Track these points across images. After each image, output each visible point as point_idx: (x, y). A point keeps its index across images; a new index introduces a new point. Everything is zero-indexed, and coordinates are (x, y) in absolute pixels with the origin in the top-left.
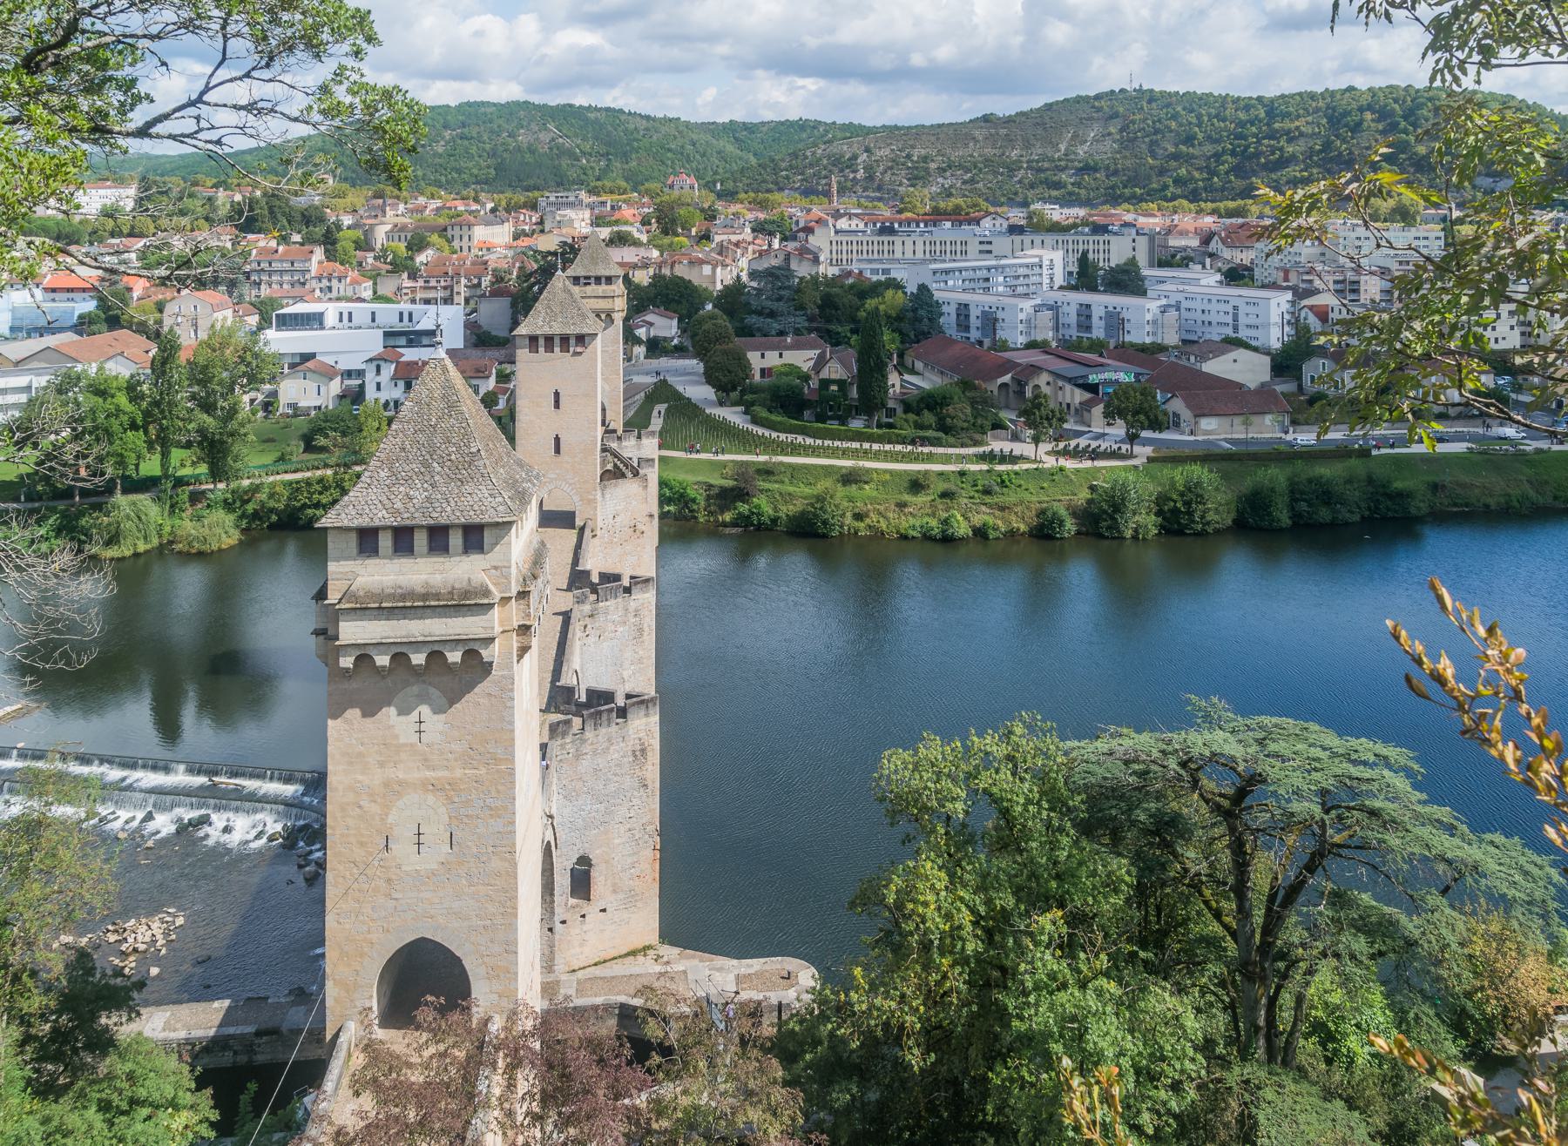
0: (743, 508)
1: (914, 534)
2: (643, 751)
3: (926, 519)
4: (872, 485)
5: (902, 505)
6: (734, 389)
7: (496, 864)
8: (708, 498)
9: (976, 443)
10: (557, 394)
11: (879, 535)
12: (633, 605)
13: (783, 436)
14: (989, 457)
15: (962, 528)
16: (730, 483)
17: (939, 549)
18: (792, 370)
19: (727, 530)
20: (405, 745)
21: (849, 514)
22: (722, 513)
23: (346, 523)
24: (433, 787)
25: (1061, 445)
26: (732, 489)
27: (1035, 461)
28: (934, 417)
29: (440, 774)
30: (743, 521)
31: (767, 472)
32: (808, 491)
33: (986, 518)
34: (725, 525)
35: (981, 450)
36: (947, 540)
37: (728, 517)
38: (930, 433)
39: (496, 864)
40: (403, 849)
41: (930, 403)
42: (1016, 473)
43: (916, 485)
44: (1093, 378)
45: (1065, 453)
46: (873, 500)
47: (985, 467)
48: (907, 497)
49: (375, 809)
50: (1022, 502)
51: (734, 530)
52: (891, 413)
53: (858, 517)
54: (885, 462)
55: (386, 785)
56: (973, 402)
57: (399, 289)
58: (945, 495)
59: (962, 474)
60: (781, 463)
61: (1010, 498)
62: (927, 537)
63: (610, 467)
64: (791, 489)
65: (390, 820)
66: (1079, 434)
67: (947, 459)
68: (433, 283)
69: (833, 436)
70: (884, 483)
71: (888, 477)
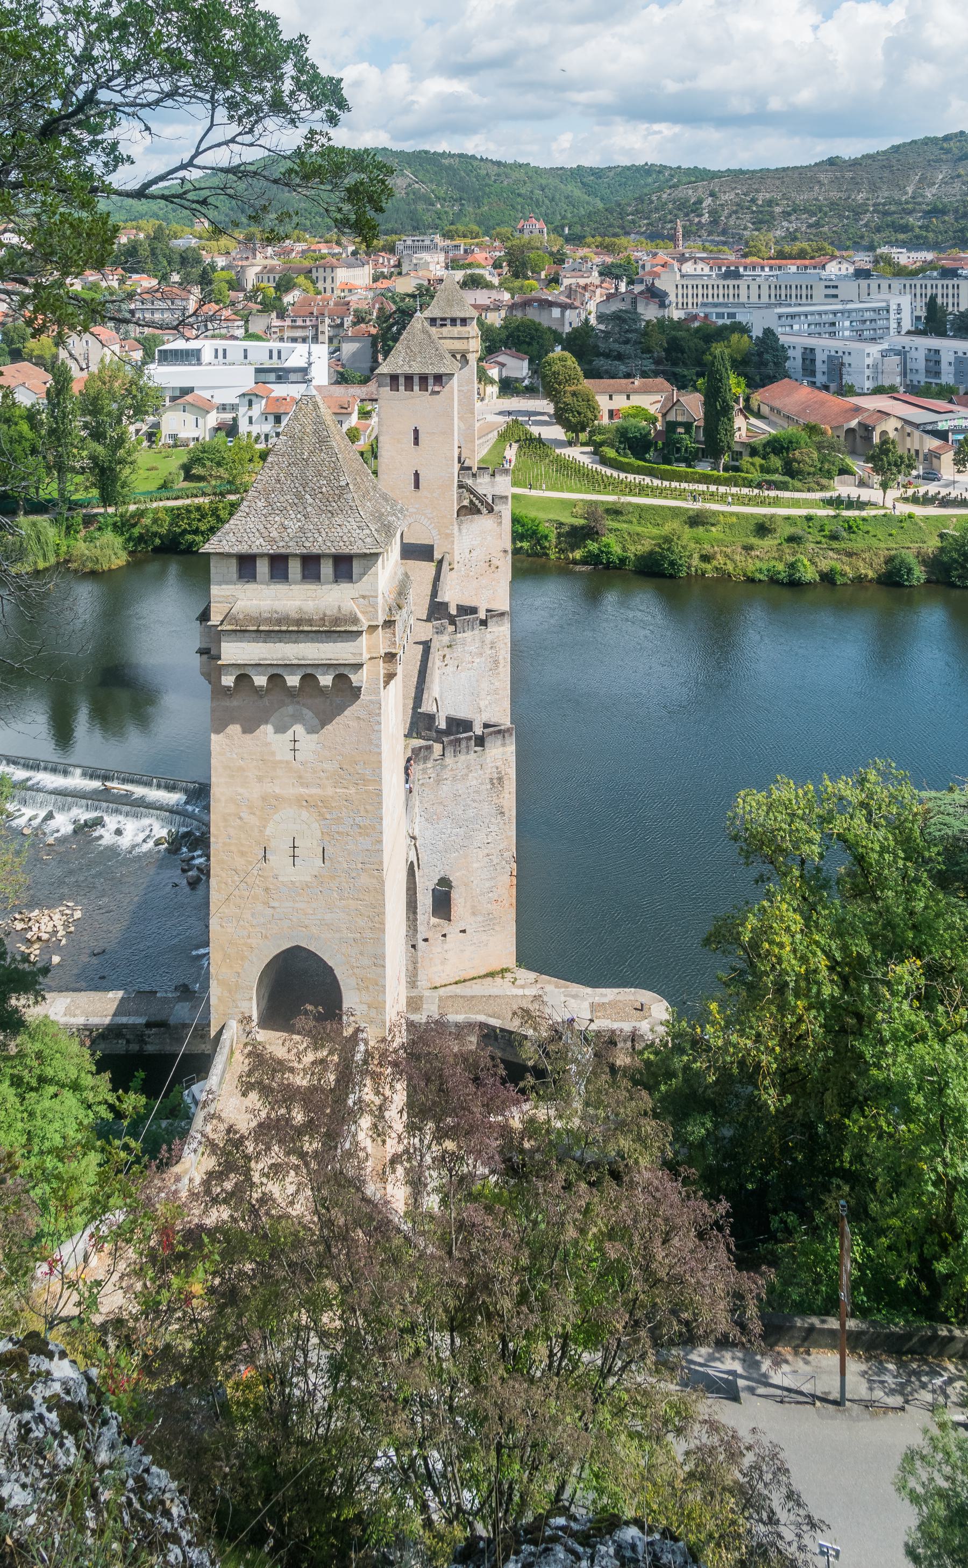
0: (593, 546)
1: (762, 577)
2: (500, 779)
3: (773, 563)
4: (719, 527)
5: (748, 548)
6: (583, 429)
7: (364, 880)
8: (559, 535)
9: (823, 488)
10: (416, 431)
11: (724, 577)
12: (489, 637)
13: (631, 477)
14: (836, 502)
15: (809, 574)
16: (582, 522)
17: (786, 594)
18: (640, 412)
19: (578, 568)
20: (281, 762)
21: (696, 556)
22: (573, 551)
23: (227, 549)
24: (305, 803)
25: (910, 492)
26: (582, 528)
27: (883, 507)
28: (784, 461)
29: (314, 791)
30: (592, 559)
31: (615, 512)
32: (655, 531)
34: (575, 562)
35: (827, 495)
36: (794, 584)
37: (578, 554)
38: (776, 477)
39: (364, 880)
40: (279, 860)
41: (777, 447)
42: (864, 519)
43: (762, 529)
44: (942, 426)
45: (915, 500)
46: (720, 543)
47: (832, 512)
49: (253, 820)
50: (870, 549)
51: (584, 568)
52: (737, 456)
53: (706, 558)
54: (731, 503)
55: (264, 799)
56: (819, 447)
58: (792, 539)
59: (809, 518)
60: (630, 504)
61: (858, 543)
62: (774, 581)
63: (466, 503)
64: (639, 529)
67: (796, 503)
69: (680, 478)
70: (731, 527)
71: (734, 520)
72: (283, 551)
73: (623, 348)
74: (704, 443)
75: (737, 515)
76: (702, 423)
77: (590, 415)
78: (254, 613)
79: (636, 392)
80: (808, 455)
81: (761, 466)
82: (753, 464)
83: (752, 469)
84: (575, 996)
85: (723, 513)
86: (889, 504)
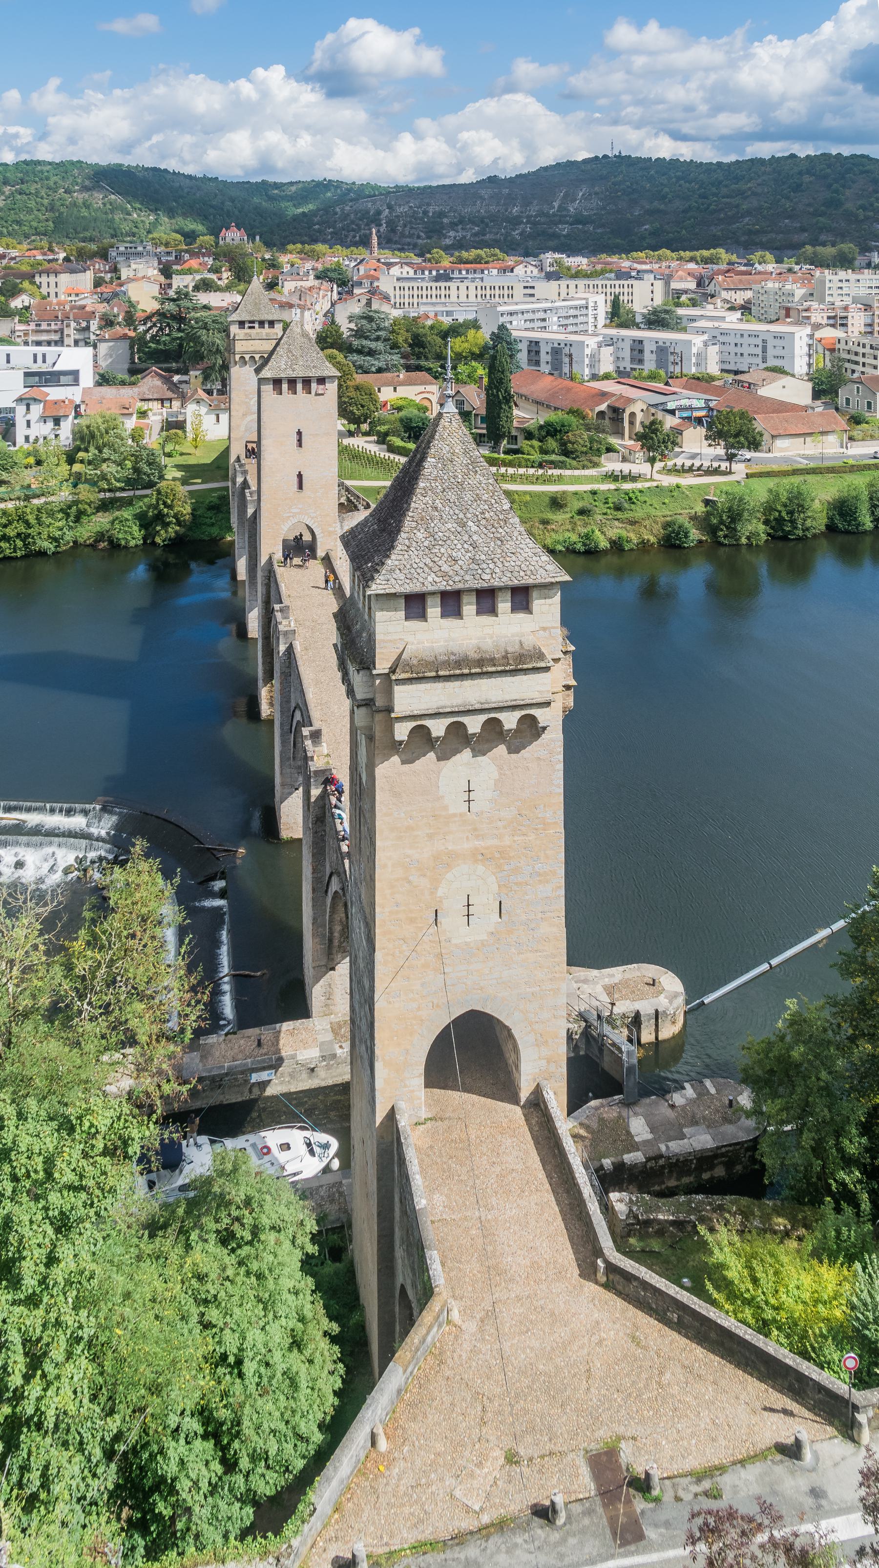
3: (567, 535)
6: (365, 422)
9: (596, 465)
14: (613, 477)
15: (604, 544)
20: (454, 815)
23: (398, 589)
24: (481, 856)
27: (651, 479)
33: (619, 531)
35: (603, 470)
38: (553, 457)
41: (550, 430)
42: (641, 491)
44: (671, 406)
47: (612, 486)
48: (550, 516)
57: (13, 332)
59: (594, 493)
61: (639, 512)
63: (343, 500)
65: (440, 893)
66: (678, 455)
68: (44, 326)
71: (528, 498)
72: (460, 586)
73: (373, 345)
74: (487, 428)
75: (530, 493)
76: (483, 412)
77: (372, 408)
78: (428, 656)
79: (402, 384)
80: (581, 437)
81: (540, 447)
82: (532, 446)
83: (533, 452)
84: (585, 981)
85: (517, 492)
86: (656, 476)
